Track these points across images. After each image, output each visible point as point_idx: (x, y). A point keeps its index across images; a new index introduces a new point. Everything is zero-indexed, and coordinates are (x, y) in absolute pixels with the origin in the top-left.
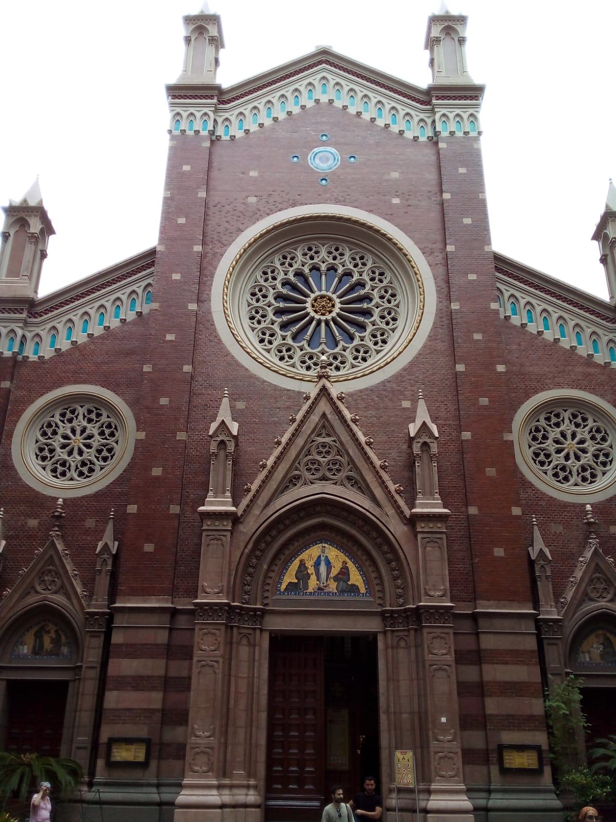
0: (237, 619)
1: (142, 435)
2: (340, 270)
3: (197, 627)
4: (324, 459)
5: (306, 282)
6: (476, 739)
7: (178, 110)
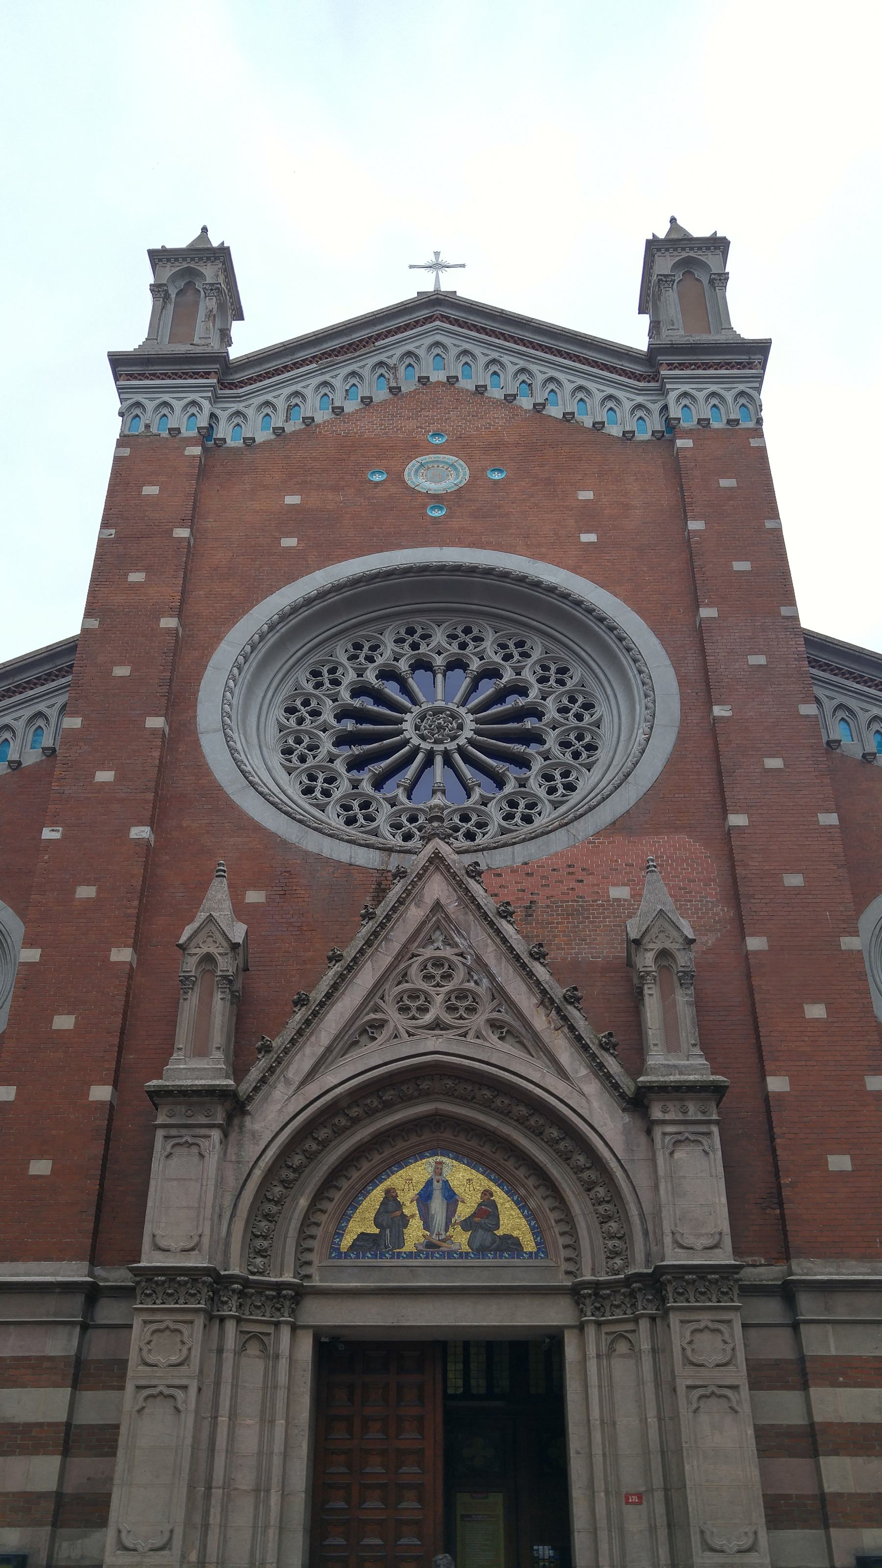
0: (234, 1303)
1: (32, 955)
2: (475, 665)
4: (438, 989)
5: (405, 690)
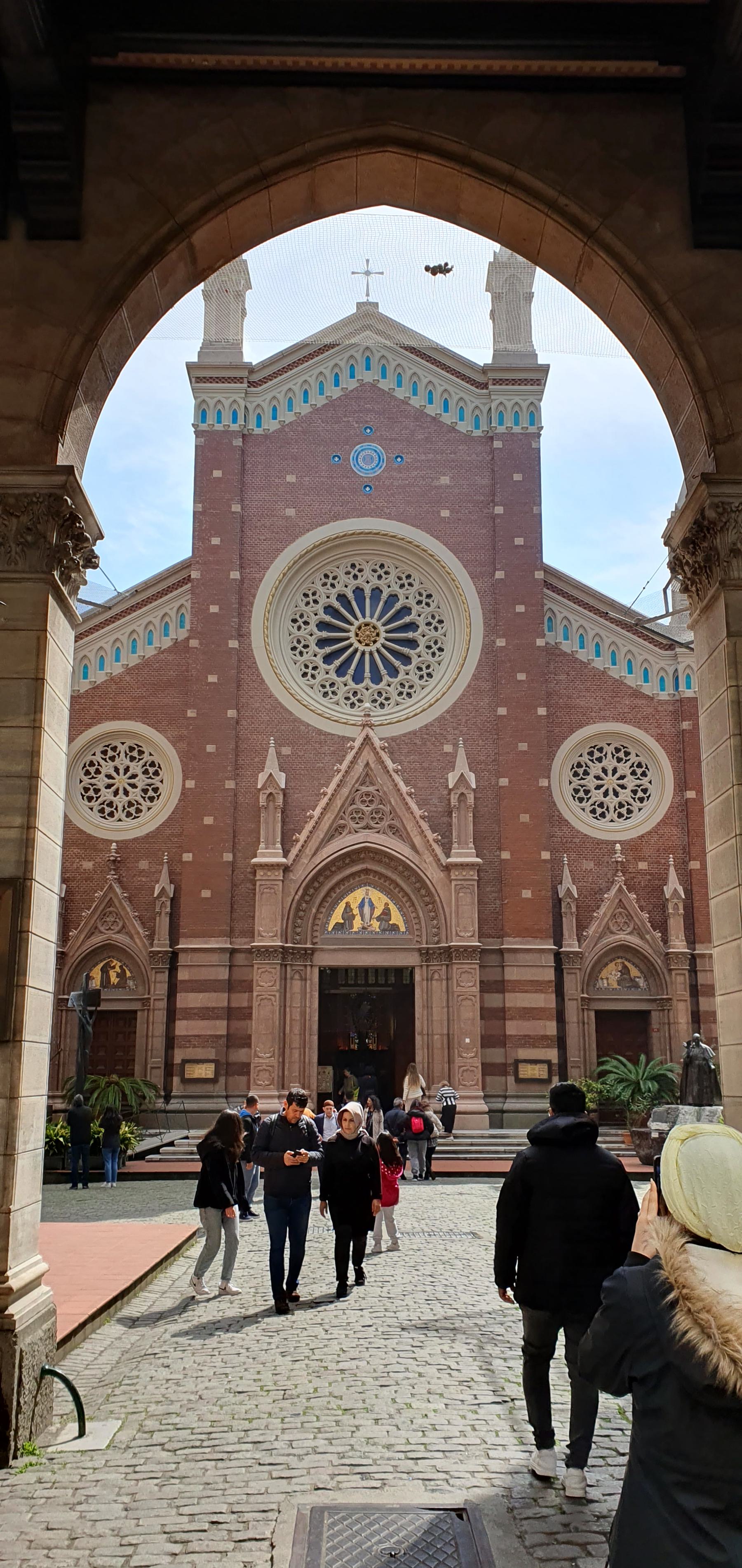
0: (289, 958)
1: (190, 784)
3: (256, 967)
6: (496, 1055)
7: (204, 396)
